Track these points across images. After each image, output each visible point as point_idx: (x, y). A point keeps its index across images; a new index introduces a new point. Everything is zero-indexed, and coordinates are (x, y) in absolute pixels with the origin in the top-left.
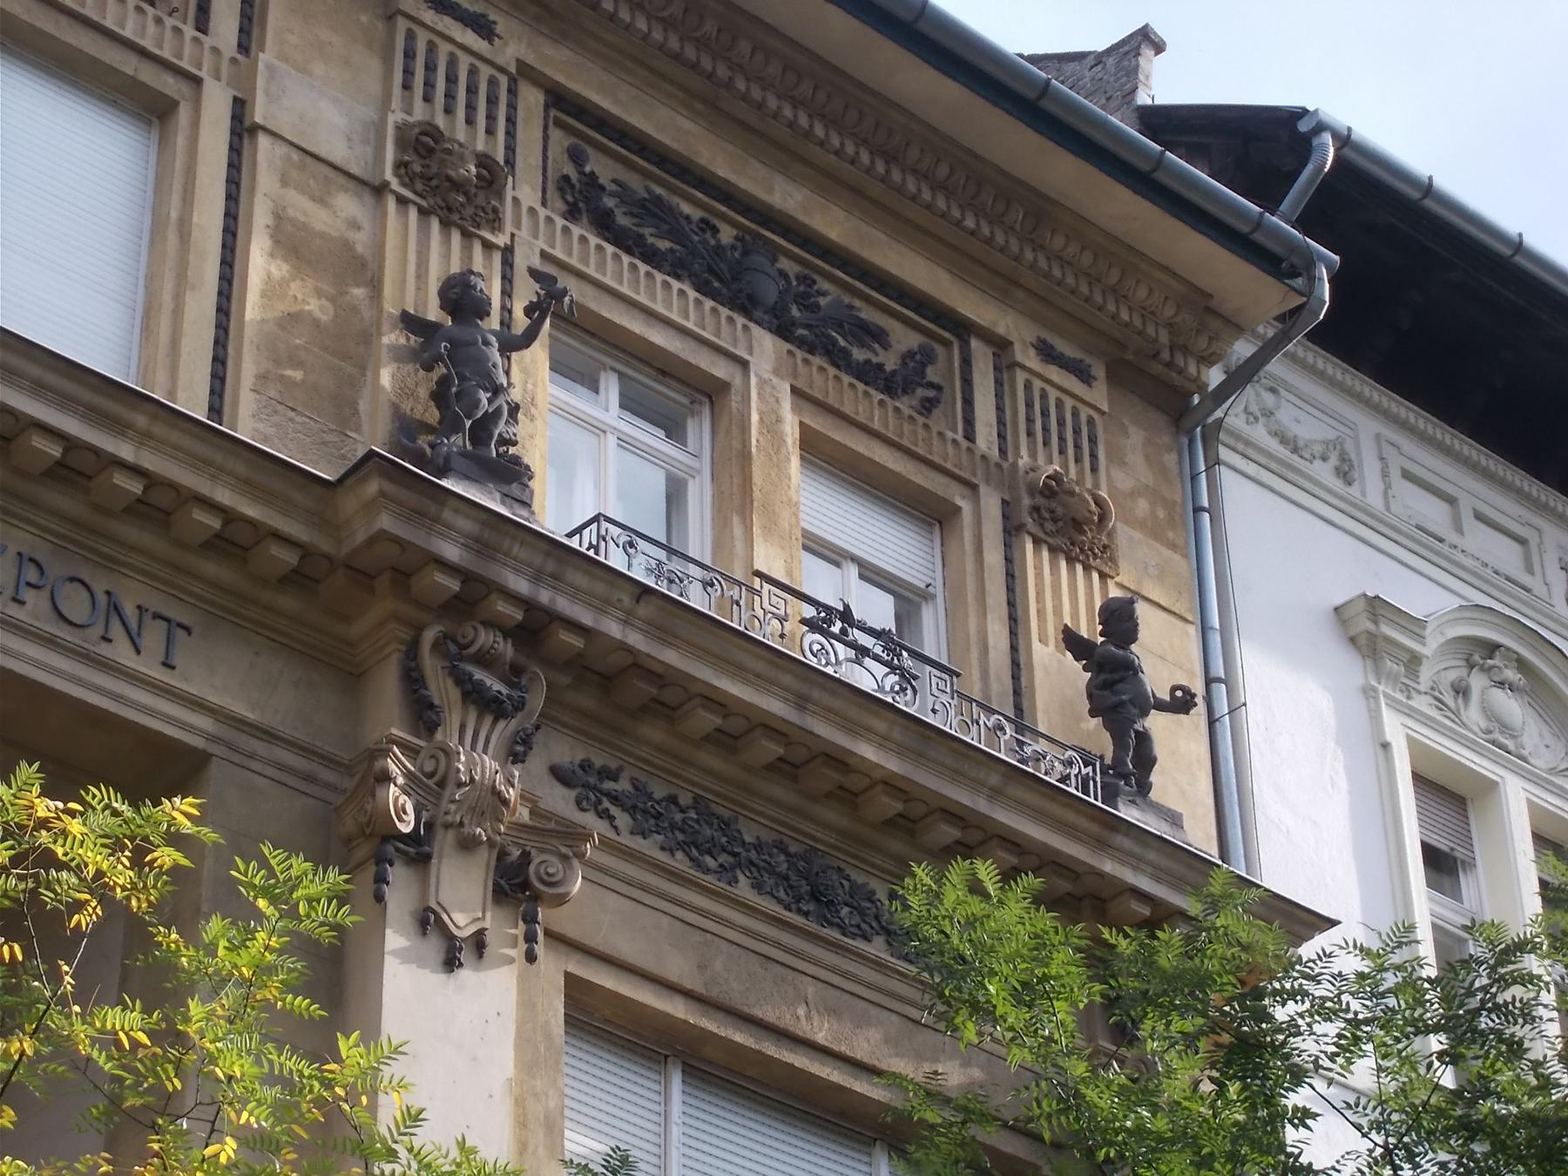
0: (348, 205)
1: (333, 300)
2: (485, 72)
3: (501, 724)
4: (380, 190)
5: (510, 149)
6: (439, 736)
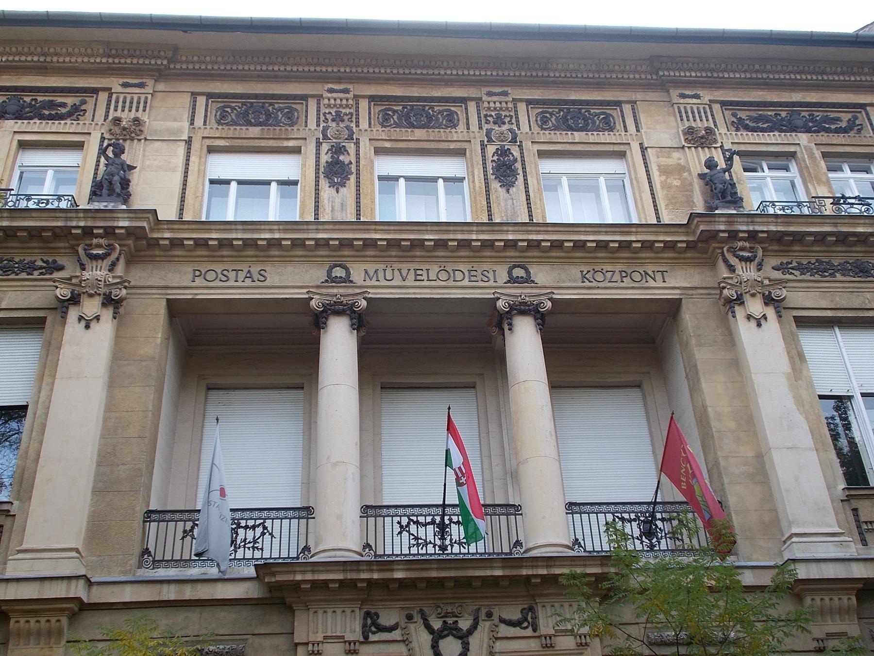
0: (676, 155)
2: (701, 107)
4: (683, 147)
5: (715, 122)
6: (737, 272)
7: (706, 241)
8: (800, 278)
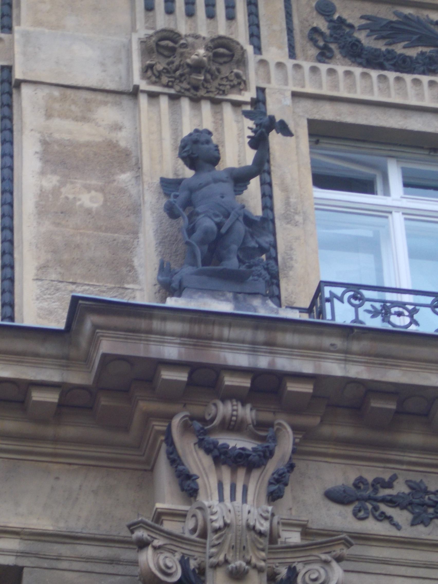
0: (109, 112)
1: (101, 190)
3: (255, 474)
4: (135, 93)
6: (202, 499)
7: (124, 391)
8: (408, 532)
